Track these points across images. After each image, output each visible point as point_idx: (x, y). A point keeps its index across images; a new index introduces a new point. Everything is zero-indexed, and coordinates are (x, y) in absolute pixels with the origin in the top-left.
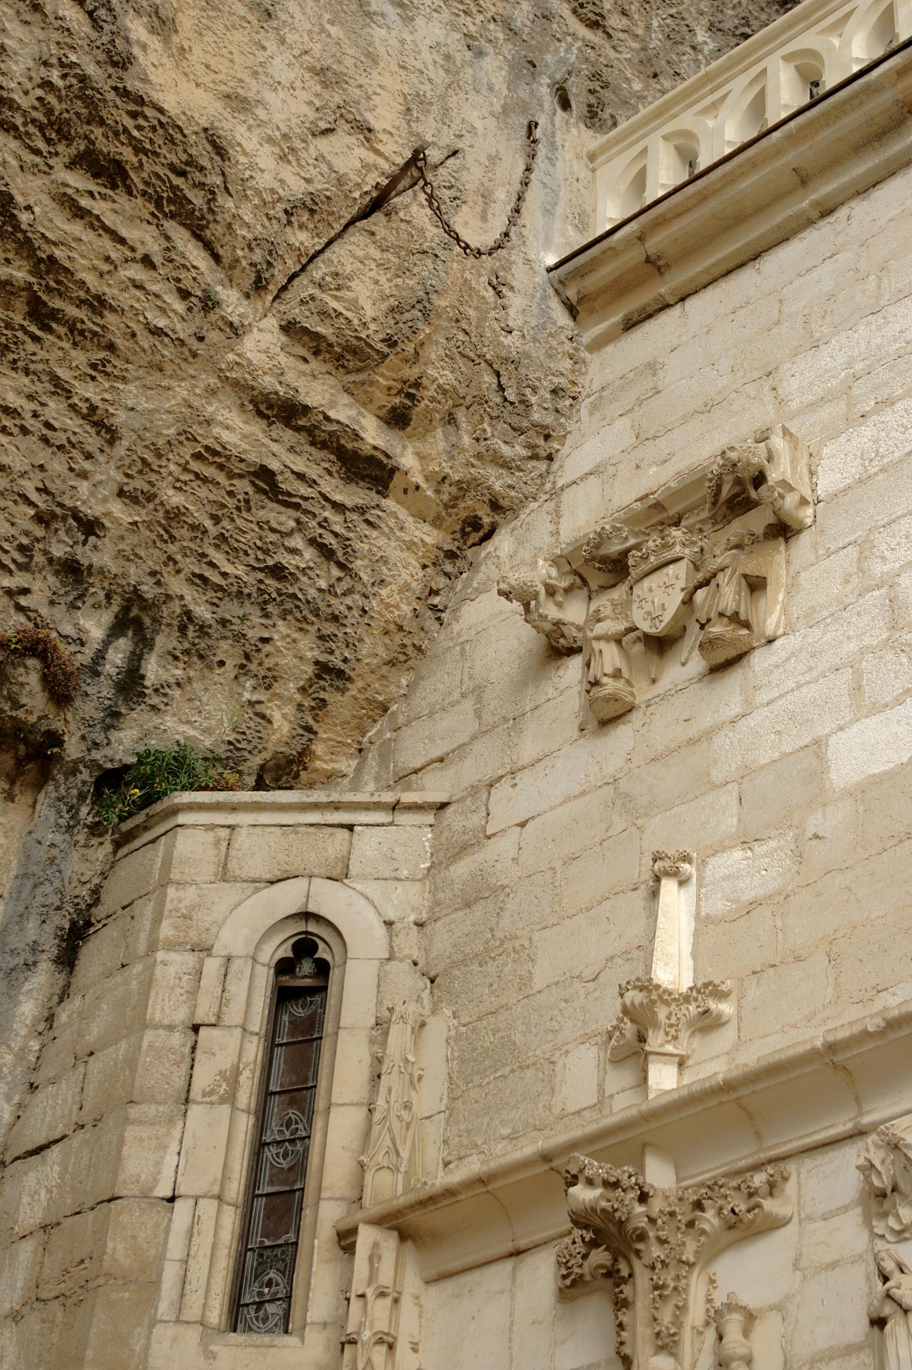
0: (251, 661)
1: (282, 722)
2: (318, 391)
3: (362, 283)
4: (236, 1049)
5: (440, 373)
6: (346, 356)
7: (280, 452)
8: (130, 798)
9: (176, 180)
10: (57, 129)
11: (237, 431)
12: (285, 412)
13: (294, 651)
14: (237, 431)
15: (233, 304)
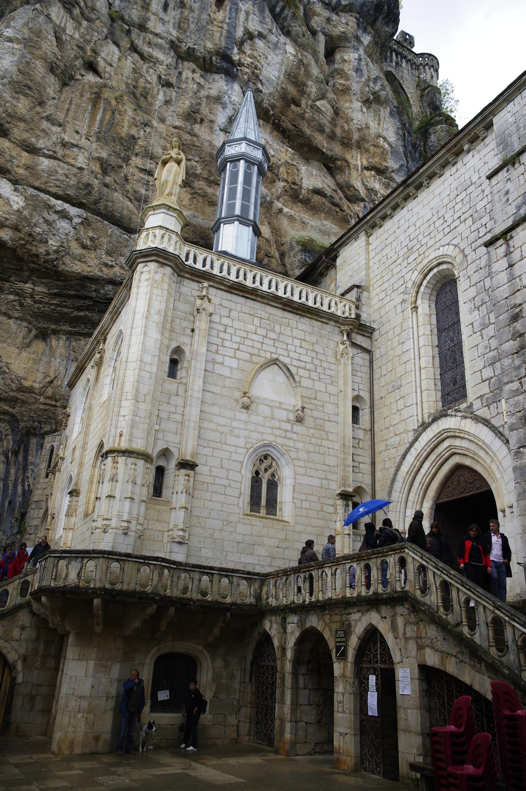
0: (50, 423)
1: (54, 427)
2: (48, 401)
3: (50, 391)
4: (47, 457)
5: (58, 397)
6: (50, 398)
7: (47, 407)
8: (42, 436)
9: (30, 390)
10: (19, 390)
11: (42, 407)
12: (45, 404)
13: (53, 421)
14: (42, 407)
15: (38, 397)
